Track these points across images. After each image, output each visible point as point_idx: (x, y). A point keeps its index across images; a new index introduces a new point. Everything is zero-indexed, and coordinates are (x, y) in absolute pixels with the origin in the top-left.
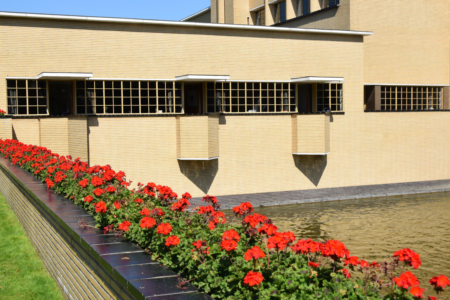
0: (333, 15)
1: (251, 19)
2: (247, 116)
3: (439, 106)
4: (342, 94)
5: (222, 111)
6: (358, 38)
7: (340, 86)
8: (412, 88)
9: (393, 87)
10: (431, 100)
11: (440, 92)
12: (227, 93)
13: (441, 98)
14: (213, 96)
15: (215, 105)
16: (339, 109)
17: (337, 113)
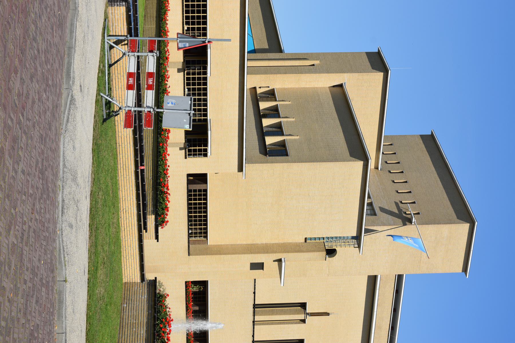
0: (261, 153)
1: (267, 89)
2: (183, 88)
3: (192, 237)
4: (199, 157)
5: (187, 70)
6: (240, 169)
7: (206, 155)
8: (206, 214)
9: (206, 199)
10: (197, 230)
11: (203, 238)
12: (199, 74)
13: (198, 238)
14: (197, 64)
15: (191, 65)
16: (189, 155)
17: (186, 153)
